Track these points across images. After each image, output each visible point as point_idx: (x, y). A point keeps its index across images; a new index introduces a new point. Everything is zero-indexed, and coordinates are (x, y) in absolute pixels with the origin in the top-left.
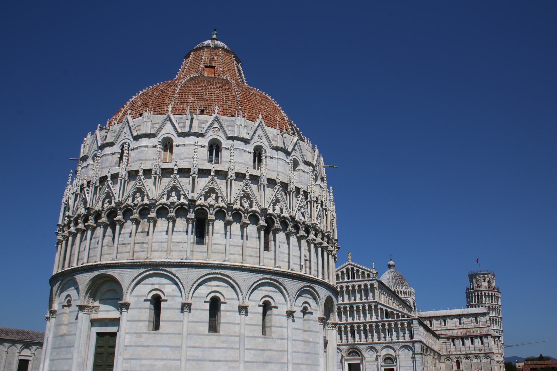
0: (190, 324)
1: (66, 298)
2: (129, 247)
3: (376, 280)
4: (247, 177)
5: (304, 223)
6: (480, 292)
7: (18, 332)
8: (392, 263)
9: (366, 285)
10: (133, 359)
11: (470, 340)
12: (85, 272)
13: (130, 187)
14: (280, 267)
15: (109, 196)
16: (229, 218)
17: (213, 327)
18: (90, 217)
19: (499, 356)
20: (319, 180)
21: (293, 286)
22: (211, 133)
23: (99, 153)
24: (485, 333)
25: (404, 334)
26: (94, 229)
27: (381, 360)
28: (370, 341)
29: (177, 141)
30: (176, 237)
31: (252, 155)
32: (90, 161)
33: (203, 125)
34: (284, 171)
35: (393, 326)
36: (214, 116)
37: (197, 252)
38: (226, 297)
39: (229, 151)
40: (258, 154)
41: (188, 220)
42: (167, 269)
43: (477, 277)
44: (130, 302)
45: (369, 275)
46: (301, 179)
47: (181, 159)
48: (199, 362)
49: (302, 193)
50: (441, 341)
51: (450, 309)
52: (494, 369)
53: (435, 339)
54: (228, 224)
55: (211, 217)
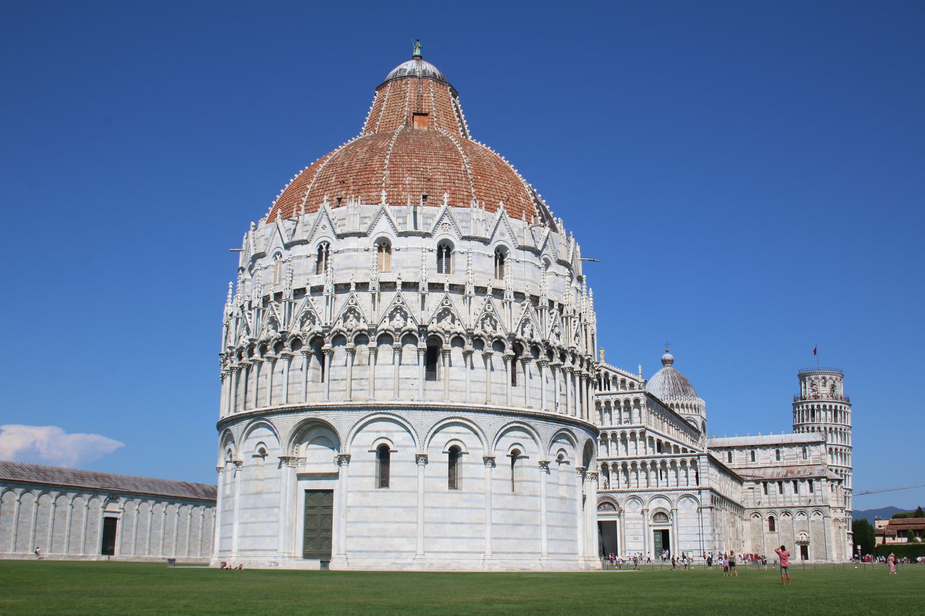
2: (343, 383)
3: (644, 392)
4: (489, 293)
5: (559, 348)
6: (816, 405)
8: (668, 356)
9: (627, 401)
11: (792, 483)
14: (531, 408)
15: (309, 316)
16: (469, 347)
18: (286, 344)
19: (839, 510)
20: (575, 280)
21: (548, 430)
23: (286, 254)
24: (816, 475)
27: (649, 516)
28: (633, 486)
29: (396, 242)
30: (404, 372)
33: (429, 221)
34: (533, 279)
36: (443, 207)
38: (468, 446)
39: (465, 256)
40: (500, 255)
44: (351, 454)
45: (632, 385)
48: (439, 525)
49: (556, 307)
50: (746, 485)
52: (829, 531)
53: (734, 483)
55: (446, 346)
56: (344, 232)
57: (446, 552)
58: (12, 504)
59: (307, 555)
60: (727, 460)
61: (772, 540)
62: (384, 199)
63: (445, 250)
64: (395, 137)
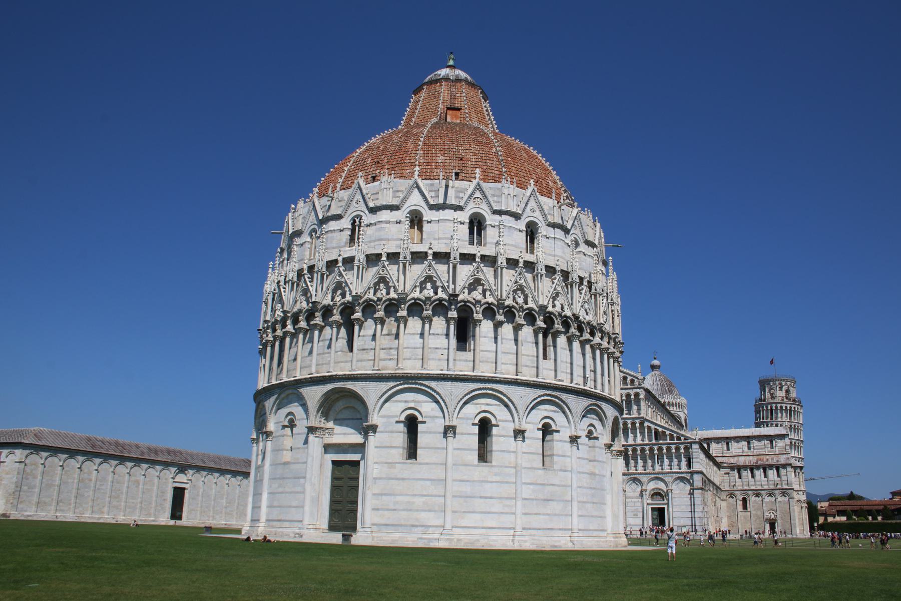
0: (456, 452)
1: (287, 416)
4: (521, 265)
5: (589, 323)
7: (169, 452)
8: (656, 362)
10: (385, 494)
11: (762, 470)
12: (315, 385)
13: (371, 274)
14: (562, 381)
15: (339, 287)
17: (483, 455)
18: (317, 314)
19: (801, 493)
21: (578, 404)
22: (471, 205)
24: (783, 462)
25: (680, 461)
26: (321, 329)
27: (647, 496)
28: (632, 470)
29: (428, 215)
31: (524, 233)
32: (306, 238)
33: (461, 195)
35: (665, 451)
36: (475, 182)
37: (460, 360)
39: (496, 229)
40: (531, 232)
41: (448, 321)
42: (426, 383)
43: (771, 383)
45: (632, 382)
46: (585, 264)
47: (435, 239)
49: (585, 283)
50: (723, 471)
51: (735, 428)
53: (715, 468)
54: (498, 325)
55: (478, 316)
56: (377, 205)
57: (475, 528)
58: (90, 473)
59: (332, 528)
61: (745, 518)
62: (417, 173)
63: (477, 225)
64: (429, 125)
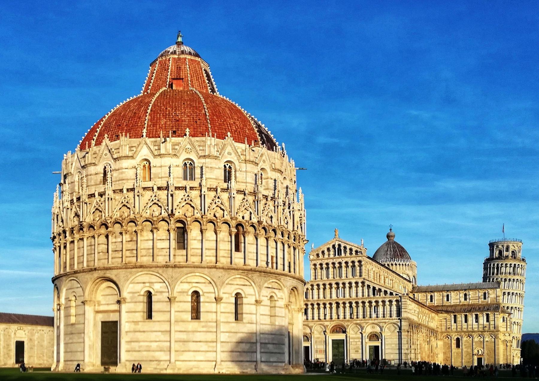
0: (177, 313)
10: (133, 342)
37: (178, 255)
48: (185, 343)
57: (190, 361)
60: (429, 300)
